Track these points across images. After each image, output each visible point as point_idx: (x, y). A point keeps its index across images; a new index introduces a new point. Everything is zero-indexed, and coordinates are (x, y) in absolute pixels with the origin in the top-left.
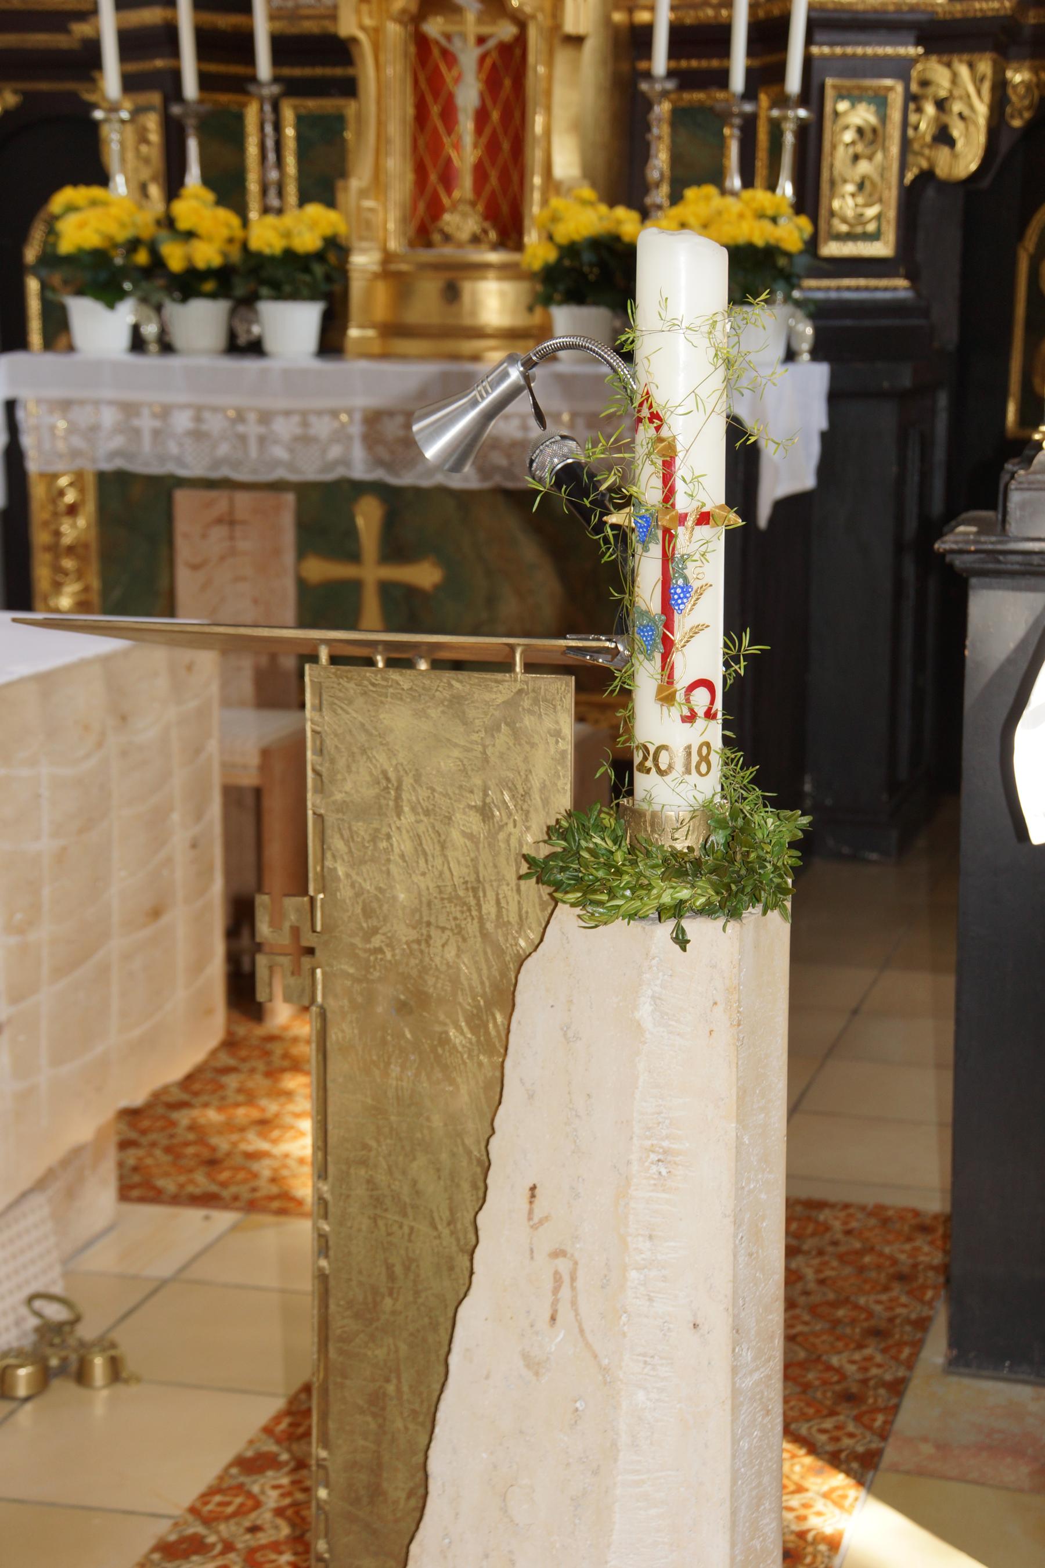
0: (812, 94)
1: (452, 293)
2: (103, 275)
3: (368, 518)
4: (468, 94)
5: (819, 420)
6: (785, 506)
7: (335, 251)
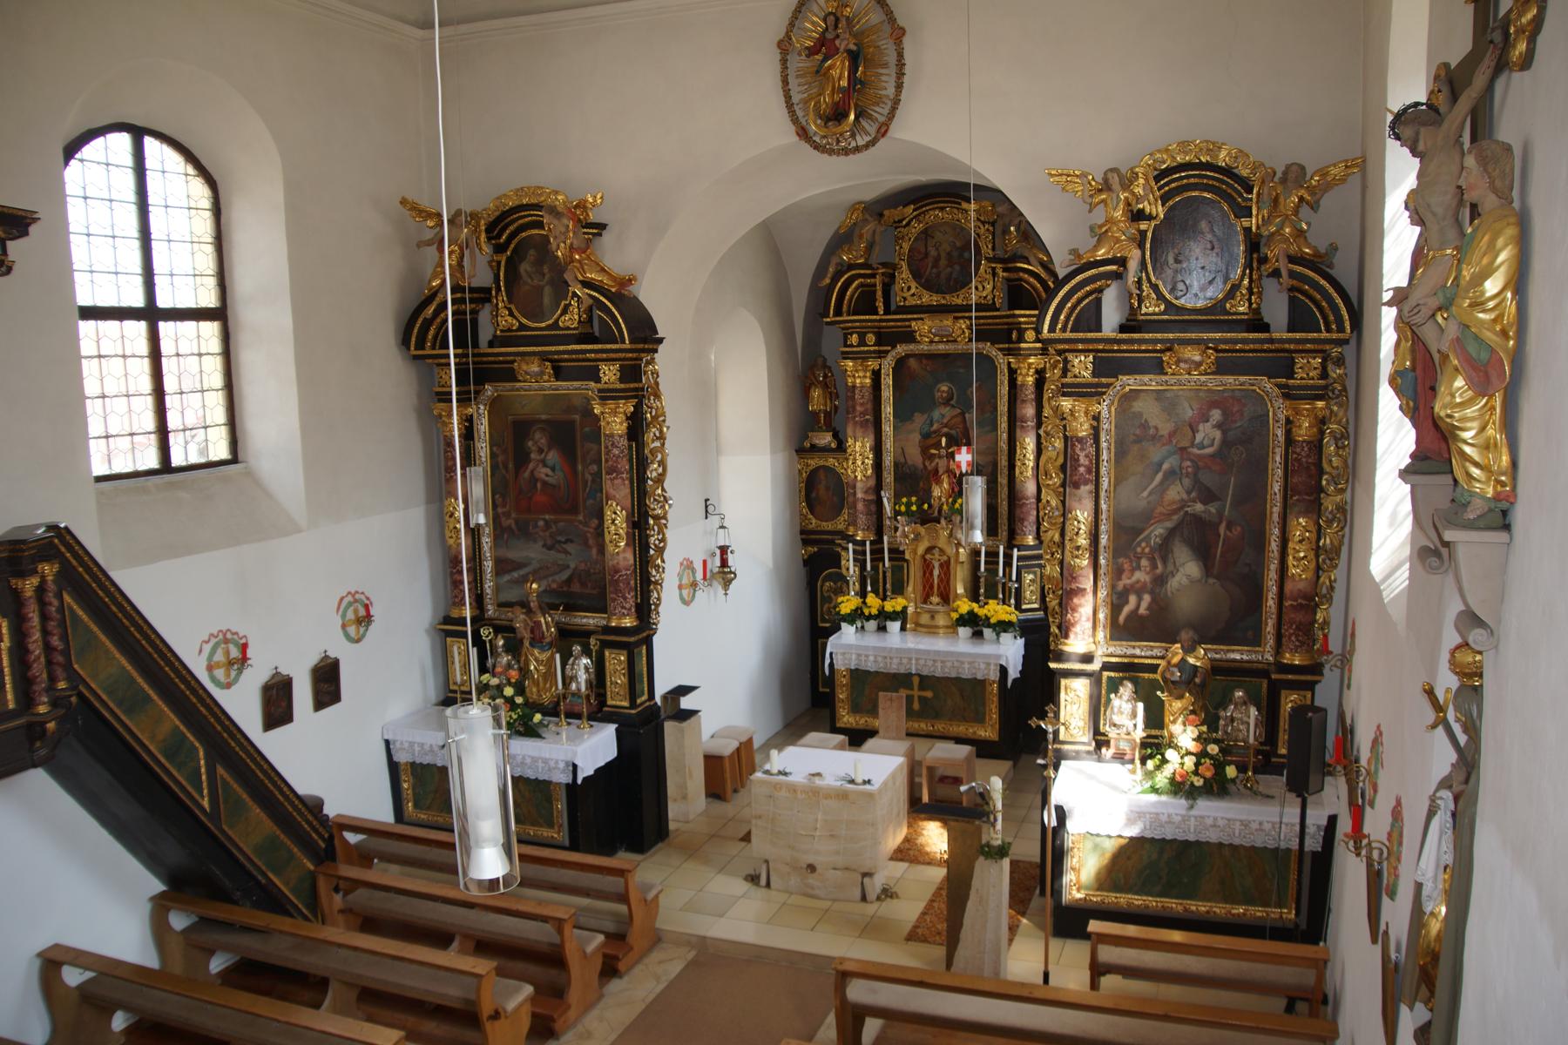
0: (1019, 579)
1: (933, 617)
2: (851, 618)
3: (916, 681)
4: (936, 572)
5: (1022, 652)
6: (1015, 680)
7: (905, 608)
